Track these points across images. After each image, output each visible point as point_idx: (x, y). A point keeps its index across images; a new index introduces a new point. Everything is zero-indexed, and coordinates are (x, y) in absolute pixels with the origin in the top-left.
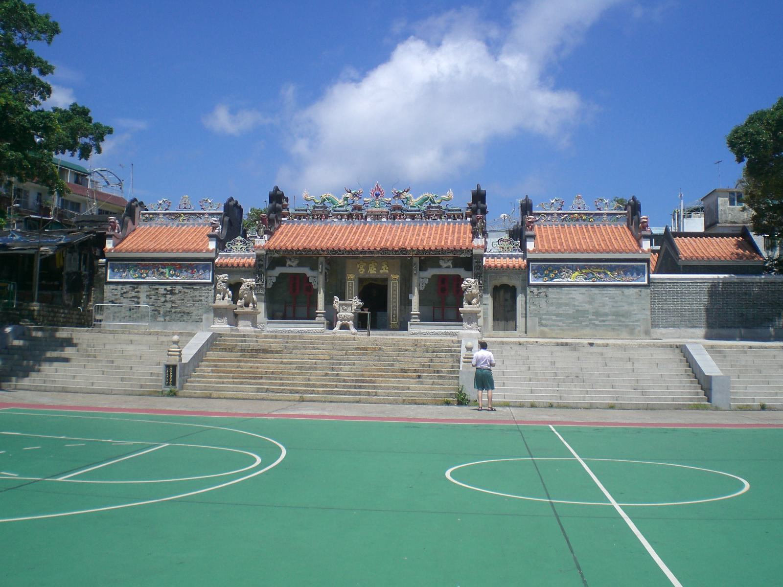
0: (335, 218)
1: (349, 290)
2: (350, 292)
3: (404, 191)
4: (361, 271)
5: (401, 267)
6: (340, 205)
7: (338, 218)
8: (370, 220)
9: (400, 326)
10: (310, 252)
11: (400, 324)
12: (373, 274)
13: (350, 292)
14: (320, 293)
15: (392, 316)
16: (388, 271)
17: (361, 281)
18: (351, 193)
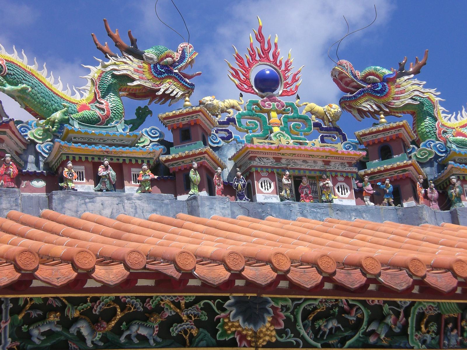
0: (80, 176)
3: (401, 74)
6: (85, 113)
7: (97, 179)
8: (275, 200)
10: (143, 317)
18: (139, 56)
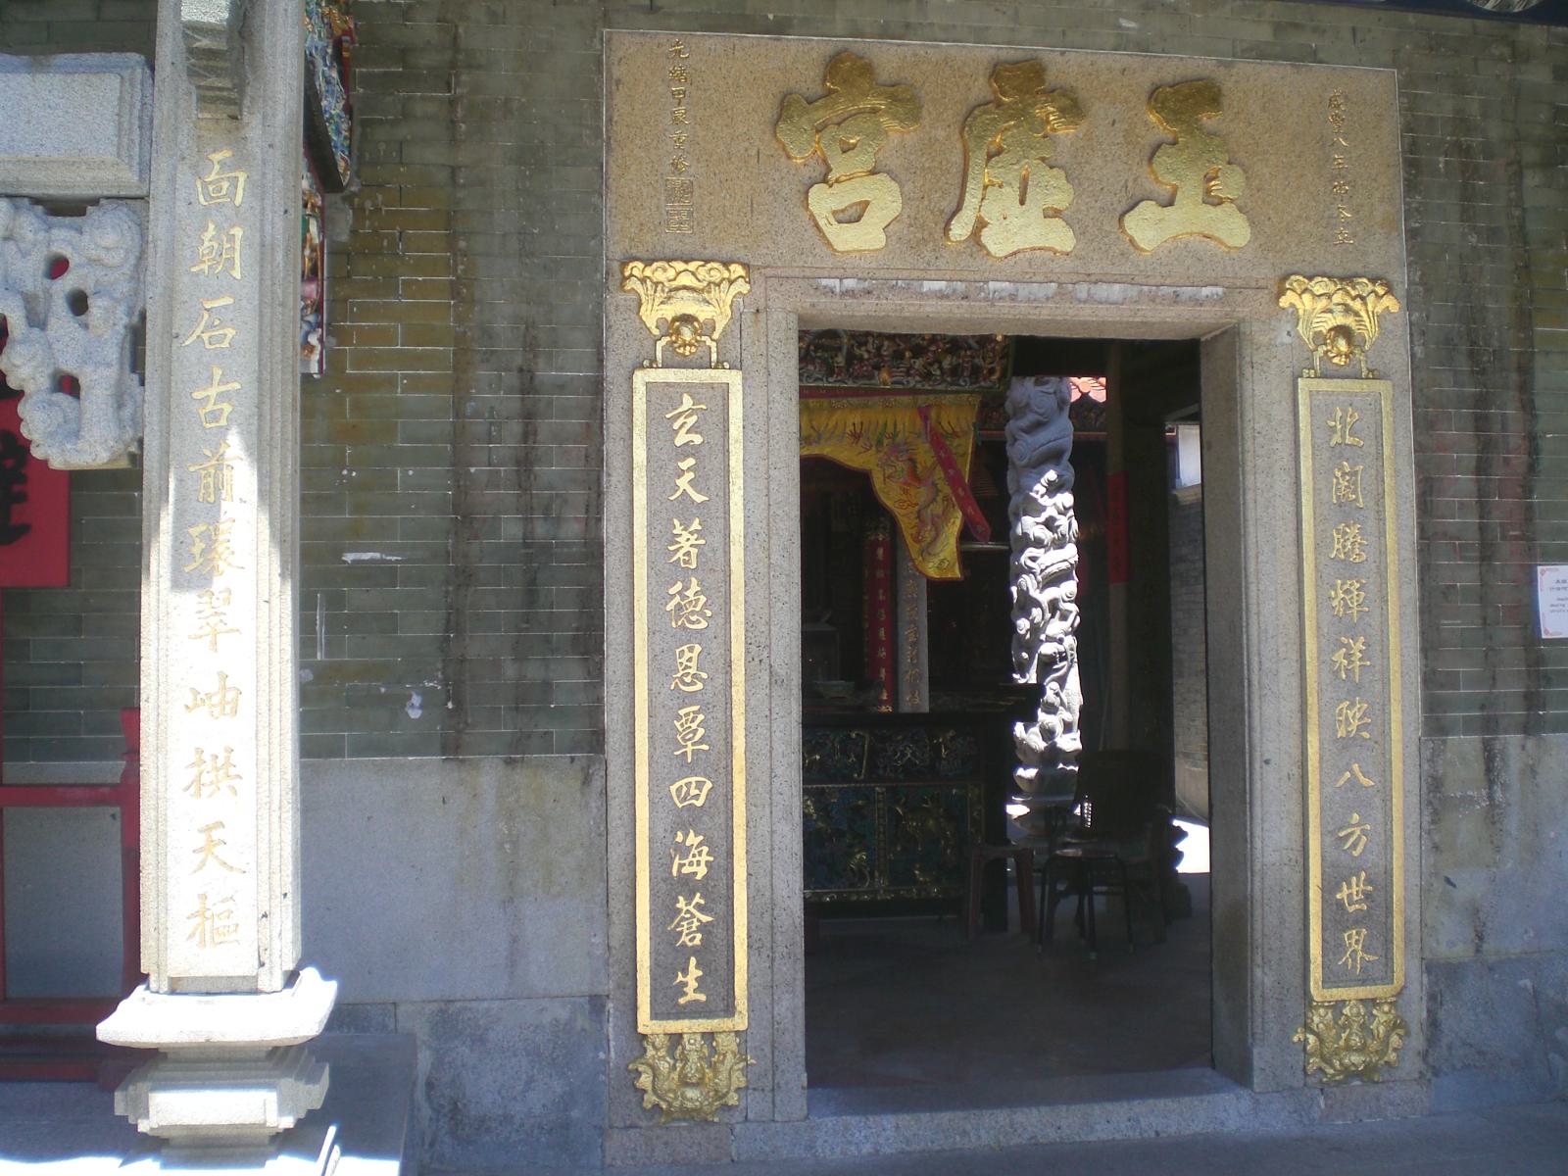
1: (668, 511)
2: (687, 542)
4: (853, 215)
5: (1414, 167)
9: (1433, 1024)
11: (1434, 999)
12: (1028, 265)
13: (687, 542)
14: (191, 576)
15: (1329, 888)
16: (1234, 230)
17: (837, 361)
